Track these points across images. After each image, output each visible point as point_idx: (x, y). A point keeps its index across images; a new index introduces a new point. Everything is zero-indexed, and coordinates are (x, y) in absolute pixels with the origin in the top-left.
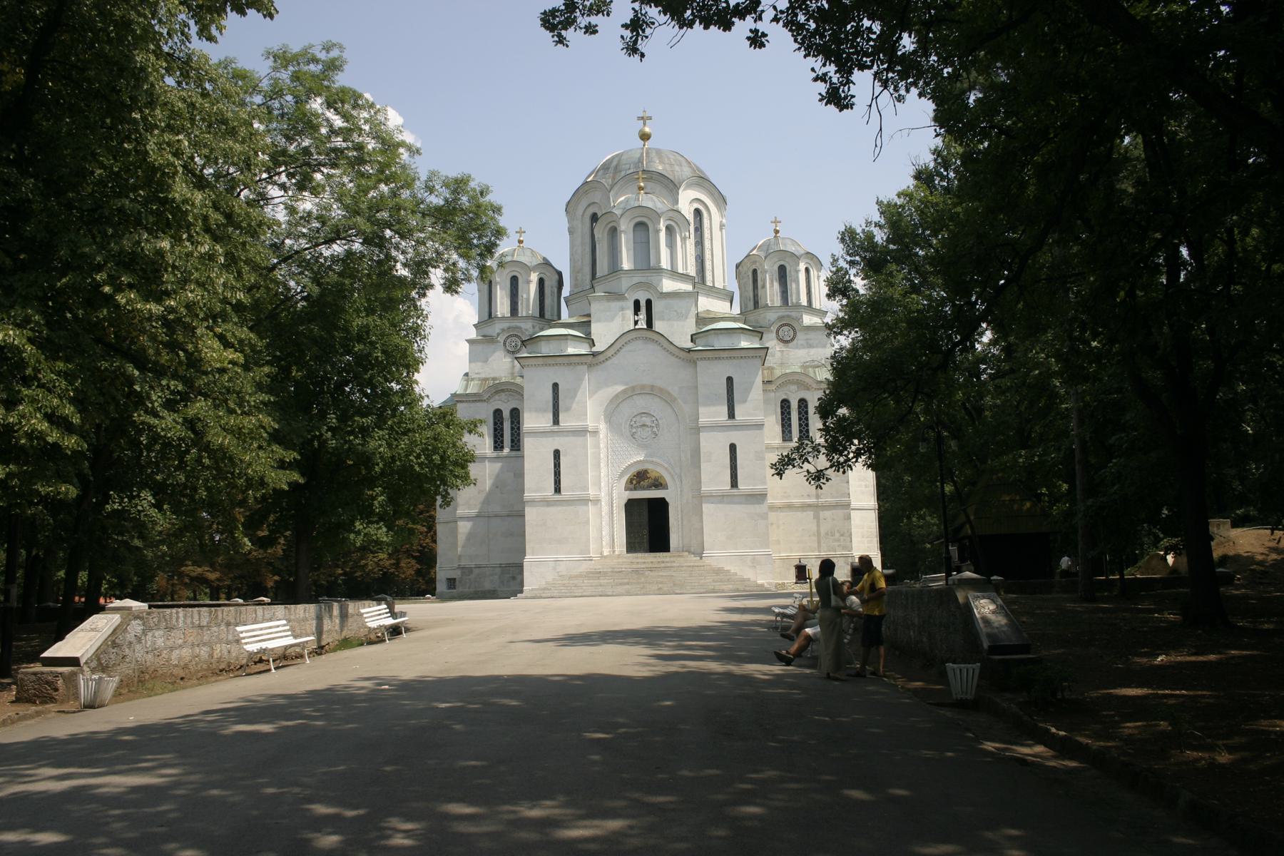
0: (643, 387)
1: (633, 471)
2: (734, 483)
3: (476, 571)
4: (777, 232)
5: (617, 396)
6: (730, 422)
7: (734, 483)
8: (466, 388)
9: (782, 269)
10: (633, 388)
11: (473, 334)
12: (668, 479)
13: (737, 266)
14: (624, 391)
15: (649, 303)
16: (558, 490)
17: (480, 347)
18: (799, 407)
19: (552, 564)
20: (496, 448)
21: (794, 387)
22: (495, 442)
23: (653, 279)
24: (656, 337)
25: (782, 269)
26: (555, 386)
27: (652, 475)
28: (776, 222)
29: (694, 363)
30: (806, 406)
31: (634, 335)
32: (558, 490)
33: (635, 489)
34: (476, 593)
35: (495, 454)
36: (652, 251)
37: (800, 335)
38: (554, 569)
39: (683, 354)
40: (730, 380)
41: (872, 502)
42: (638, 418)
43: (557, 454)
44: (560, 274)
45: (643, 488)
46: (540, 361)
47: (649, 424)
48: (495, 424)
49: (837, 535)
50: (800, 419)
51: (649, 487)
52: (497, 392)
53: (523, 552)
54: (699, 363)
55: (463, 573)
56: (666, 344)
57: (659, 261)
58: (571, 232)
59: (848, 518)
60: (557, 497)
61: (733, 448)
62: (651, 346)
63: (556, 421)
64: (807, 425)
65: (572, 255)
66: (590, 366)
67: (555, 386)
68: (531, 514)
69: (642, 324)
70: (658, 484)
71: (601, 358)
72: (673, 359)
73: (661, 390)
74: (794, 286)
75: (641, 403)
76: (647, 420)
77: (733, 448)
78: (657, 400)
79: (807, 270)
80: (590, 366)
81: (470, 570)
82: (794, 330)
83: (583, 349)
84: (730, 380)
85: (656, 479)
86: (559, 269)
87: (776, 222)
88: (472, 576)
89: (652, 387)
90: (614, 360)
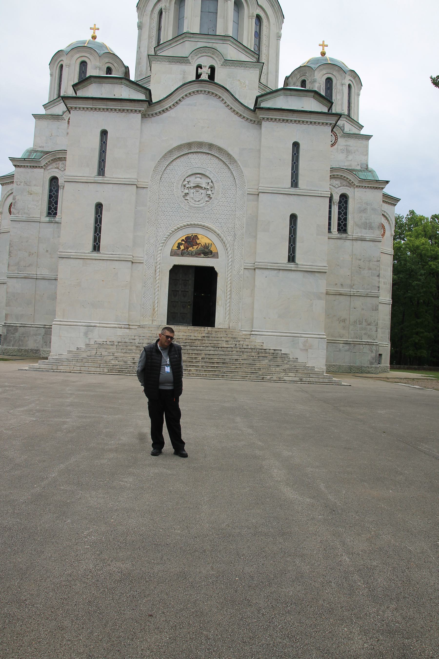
0: (200, 144)
1: (181, 235)
2: (292, 258)
3: (21, 330)
4: (323, 54)
5: (171, 152)
6: (293, 190)
7: (292, 258)
8: (29, 155)
9: (329, 81)
10: (189, 145)
11: (43, 111)
12: (218, 247)
13: (287, 78)
14: (179, 147)
15: (212, 69)
16: (96, 248)
17: (44, 123)
18: (340, 202)
19: (83, 329)
20: (49, 214)
21: (337, 182)
22: (49, 208)
23: (220, 46)
24: (219, 92)
25: (329, 81)
26: (104, 133)
27: (203, 241)
28: (323, 45)
29: (259, 123)
30: (346, 202)
31: (196, 87)
32: (96, 248)
33: (182, 255)
34: (19, 350)
35: (47, 219)
36: (220, 21)
37: (341, 141)
38: (86, 334)
39: (246, 114)
40: (296, 145)
41: (386, 297)
42: (192, 179)
43: (99, 207)
44: (127, 68)
45: (191, 255)
46: (89, 104)
47: (204, 186)
48: (51, 191)
49: (364, 323)
50: (339, 213)
51: (197, 254)
52: (54, 160)
53: (53, 313)
54: (264, 124)
55: (8, 331)
56: (229, 100)
57: (226, 29)
58: (140, 27)
59: (377, 309)
60: (95, 255)
61: (293, 218)
62: (214, 102)
63: (101, 171)
64: (345, 219)
65: (139, 47)
66: (145, 116)
67: (104, 133)
68: (65, 270)
69: (205, 77)
70: (207, 252)
71: (158, 109)
72: (236, 118)
73: (220, 149)
74: (339, 97)
75: (197, 162)
76: (203, 182)
77: (293, 218)
78: (217, 161)
79: (349, 86)
80: (145, 116)
81: (16, 328)
82: (336, 136)
83: (142, 97)
84: (296, 145)
85: (206, 247)
86: (126, 64)
87: (323, 45)
88: (17, 335)
89: (211, 146)
90: (171, 113)
